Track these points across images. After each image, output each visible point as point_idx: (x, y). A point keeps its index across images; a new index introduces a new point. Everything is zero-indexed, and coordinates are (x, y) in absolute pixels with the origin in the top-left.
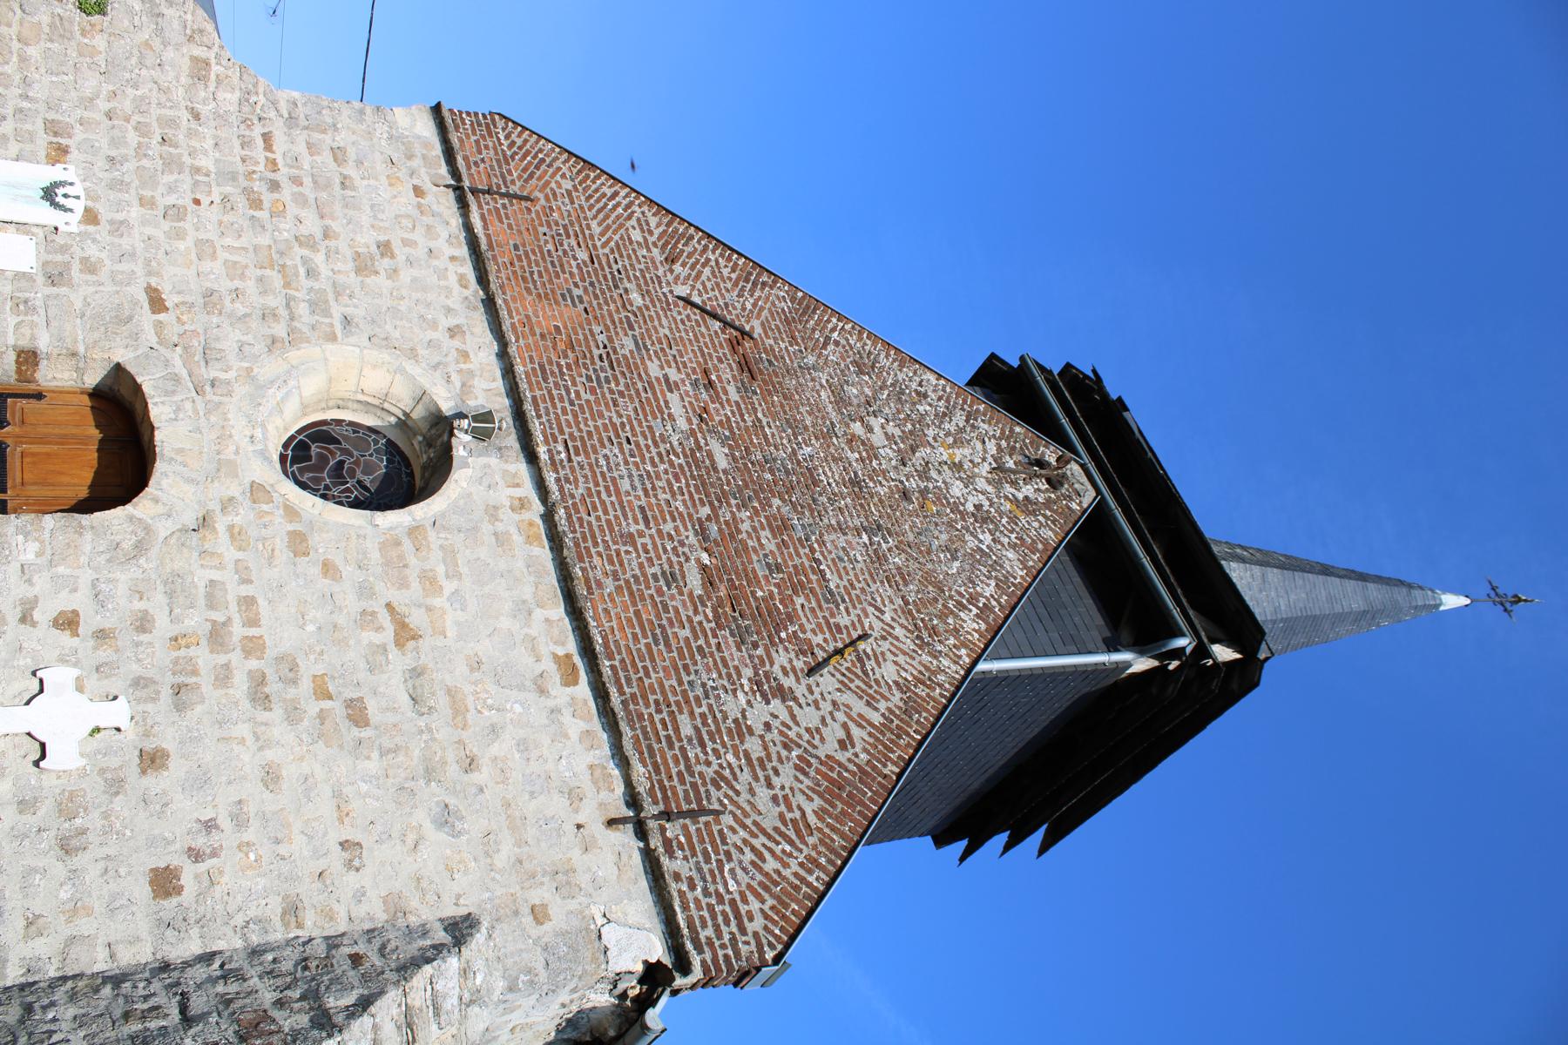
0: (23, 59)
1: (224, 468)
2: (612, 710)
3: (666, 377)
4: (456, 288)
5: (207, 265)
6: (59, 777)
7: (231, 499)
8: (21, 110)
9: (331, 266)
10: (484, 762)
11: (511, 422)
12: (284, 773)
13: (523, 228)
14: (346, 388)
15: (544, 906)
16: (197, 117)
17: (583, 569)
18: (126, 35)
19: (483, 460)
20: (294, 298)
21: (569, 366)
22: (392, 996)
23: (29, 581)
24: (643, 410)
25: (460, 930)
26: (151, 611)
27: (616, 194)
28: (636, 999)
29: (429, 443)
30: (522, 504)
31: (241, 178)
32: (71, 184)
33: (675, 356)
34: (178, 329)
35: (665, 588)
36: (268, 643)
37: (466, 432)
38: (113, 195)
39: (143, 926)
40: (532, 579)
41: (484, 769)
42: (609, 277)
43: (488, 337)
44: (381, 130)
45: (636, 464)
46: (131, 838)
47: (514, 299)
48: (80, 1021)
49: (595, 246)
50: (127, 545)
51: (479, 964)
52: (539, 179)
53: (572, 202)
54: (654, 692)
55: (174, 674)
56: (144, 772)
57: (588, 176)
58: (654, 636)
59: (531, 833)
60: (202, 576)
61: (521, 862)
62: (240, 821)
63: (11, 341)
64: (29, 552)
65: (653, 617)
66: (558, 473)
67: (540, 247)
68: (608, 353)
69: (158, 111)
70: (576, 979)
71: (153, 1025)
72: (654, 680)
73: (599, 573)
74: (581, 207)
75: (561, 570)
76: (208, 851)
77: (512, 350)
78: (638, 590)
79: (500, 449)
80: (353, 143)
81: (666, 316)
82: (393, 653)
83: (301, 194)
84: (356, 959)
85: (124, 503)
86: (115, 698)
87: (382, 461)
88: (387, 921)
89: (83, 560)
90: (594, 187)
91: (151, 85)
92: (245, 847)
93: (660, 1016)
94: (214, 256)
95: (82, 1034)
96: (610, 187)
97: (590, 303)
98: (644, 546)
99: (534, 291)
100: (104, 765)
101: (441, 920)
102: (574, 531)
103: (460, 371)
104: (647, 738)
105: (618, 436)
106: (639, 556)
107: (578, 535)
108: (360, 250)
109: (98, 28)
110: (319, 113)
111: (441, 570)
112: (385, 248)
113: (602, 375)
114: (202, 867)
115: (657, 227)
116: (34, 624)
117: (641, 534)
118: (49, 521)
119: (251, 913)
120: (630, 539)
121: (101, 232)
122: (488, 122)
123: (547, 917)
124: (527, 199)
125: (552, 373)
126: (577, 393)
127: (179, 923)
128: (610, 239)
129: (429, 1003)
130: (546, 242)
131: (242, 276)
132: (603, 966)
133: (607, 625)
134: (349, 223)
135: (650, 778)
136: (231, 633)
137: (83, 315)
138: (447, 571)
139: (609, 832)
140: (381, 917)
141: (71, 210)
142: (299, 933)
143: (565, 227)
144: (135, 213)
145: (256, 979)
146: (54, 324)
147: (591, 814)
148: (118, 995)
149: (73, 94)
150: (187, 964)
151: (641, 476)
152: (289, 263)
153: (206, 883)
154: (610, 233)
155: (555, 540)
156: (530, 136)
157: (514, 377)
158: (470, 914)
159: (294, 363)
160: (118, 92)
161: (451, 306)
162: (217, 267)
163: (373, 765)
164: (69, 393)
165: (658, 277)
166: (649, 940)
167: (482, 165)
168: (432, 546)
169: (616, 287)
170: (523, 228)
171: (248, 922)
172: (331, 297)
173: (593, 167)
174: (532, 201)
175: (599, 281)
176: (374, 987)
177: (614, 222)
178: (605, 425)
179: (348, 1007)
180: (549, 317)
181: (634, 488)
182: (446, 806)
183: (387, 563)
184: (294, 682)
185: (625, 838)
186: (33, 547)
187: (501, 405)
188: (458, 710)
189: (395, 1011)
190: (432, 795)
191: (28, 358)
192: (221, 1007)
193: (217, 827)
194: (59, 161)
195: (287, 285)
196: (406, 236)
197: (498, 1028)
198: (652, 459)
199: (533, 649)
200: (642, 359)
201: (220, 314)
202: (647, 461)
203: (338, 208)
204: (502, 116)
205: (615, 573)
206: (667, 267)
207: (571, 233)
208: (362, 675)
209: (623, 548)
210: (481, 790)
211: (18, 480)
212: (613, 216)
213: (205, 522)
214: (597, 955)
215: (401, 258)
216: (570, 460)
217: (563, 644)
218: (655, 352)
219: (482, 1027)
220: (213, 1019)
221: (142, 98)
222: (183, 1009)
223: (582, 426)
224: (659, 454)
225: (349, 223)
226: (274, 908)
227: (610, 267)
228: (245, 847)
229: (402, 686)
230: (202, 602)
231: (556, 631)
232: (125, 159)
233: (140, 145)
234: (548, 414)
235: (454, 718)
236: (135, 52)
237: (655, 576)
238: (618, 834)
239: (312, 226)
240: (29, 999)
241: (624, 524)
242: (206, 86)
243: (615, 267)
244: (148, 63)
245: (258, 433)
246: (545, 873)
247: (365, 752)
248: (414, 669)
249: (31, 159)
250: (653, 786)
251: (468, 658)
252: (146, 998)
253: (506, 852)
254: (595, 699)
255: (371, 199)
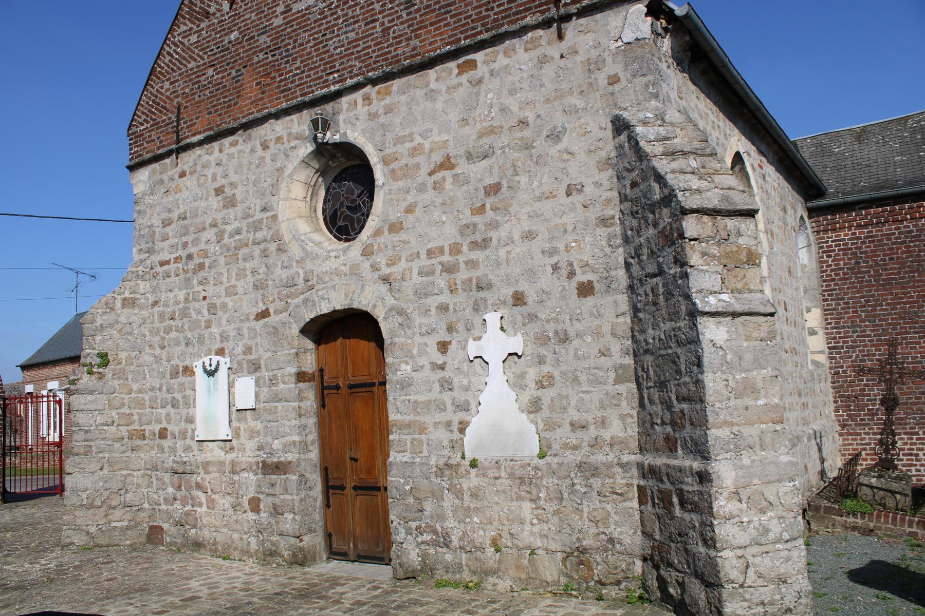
0: (140, 391)
1: (354, 271)
2: (491, 38)
3: (282, 13)
4: (239, 147)
5: (240, 290)
6: (527, 346)
7: (372, 266)
8: (168, 390)
9: (233, 221)
10: (522, 115)
11: (317, 108)
12: (527, 229)
13: (197, 110)
14: (304, 208)
15: (609, 77)
16: (156, 303)
17: (405, 60)
18: (117, 342)
19: (341, 124)
20: (254, 240)
21: (281, 75)
22: (655, 163)
23: (422, 367)
24: (304, 26)
25: (620, 126)
26: (436, 305)
27: (169, 53)
28: (668, 22)
29: (333, 157)
30: (367, 99)
31: (188, 276)
32: (204, 363)
33: (269, 9)
34: (277, 302)
35: (416, 7)
36: (453, 241)
37: (325, 135)
38: (207, 342)
39: (609, 299)
40: (412, 90)
41: (527, 114)
42: (222, 54)
43: (266, 125)
44: (148, 200)
45: (338, 30)
46: (561, 308)
47: (242, 112)
48: (655, 326)
49: (204, 64)
50: (400, 320)
51: (641, 115)
52: (165, 102)
53: (178, 81)
54: (481, 12)
55: (471, 291)
56: (525, 303)
57: (160, 72)
58: (446, 13)
59: (565, 86)
60: (416, 279)
61: (582, 92)
62: (553, 252)
63: (293, 385)
64: (406, 368)
65: (434, 15)
66: (347, 78)
67: (208, 99)
68: (270, 51)
69: (156, 323)
70: (654, 58)
71: (661, 290)
72: (473, 12)
73: (407, 49)
74: (180, 75)
75: (406, 73)
76: (570, 268)
77: (273, 110)
78: (417, 24)
79: (334, 114)
80: (159, 215)
81: (244, 16)
82: (458, 170)
83: (193, 242)
84: (634, 185)
85: (377, 323)
86: (485, 320)
87: (345, 184)
88: (613, 169)
89: (409, 341)
90: (166, 68)
91: (142, 328)
92: (568, 249)
93: (679, 6)
94: (234, 286)
95: (662, 325)
96: (165, 57)
97: (239, 65)
98: (389, 22)
99: (236, 100)
100: (521, 323)
101: (614, 139)
102: (382, 66)
103: (289, 141)
104: (509, 16)
105: (322, 42)
106: (396, 25)
107: (384, 63)
108: (222, 205)
109: (115, 356)
110: (143, 236)
111: (408, 145)
112: (219, 191)
113: (284, 54)
114: (578, 271)
115: (186, 25)
116: (445, 363)
117: (382, 24)
118: (389, 360)
119: (605, 243)
120: (385, 31)
121: (228, 346)
122: (135, 137)
123: (616, 75)
124: (179, 109)
125: (285, 85)
126: (296, 69)
127: (608, 281)
128: (198, 55)
129: (661, 143)
130: (204, 95)
131: (244, 270)
132: (647, 41)
133: (439, 43)
134: (206, 213)
135: (534, 13)
136: (448, 262)
137: (275, 351)
138: (409, 141)
139: (566, 38)
140: (611, 172)
141: (218, 362)
142: (617, 217)
143: (194, 84)
144: (215, 330)
145: (641, 239)
146: (281, 365)
147: (554, 51)
148: (644, 310)
149: (154, 366)
150: (630, 276)
151: (346, 26)
152: (233, 245)
153: (587, 268)
154: (194, 55)
155: (388, 77)
156: (139, 110)
157: (290, 108)
158: (611, 121)
159: (291, 237)
160: (149, 344)
161: (249, 149)
162: (240, 285)
163: (523, 179)
164: (318, 356)
165: (219, 22)
166: (633, 13)
167: (161, 138)
168: (394, 151)
169: (228, 49)
170: (197, 110)
171: (610, 245)
172: (251, 220)
173: (153, 69)
174: (180, 106)
175: (226, 60)
176: (651, 173)
177: (187, 53)
178: (315, 51)
179: (660, 188)
180: (251, 90)
181: (354, 30)
182: (547, 136)
183: (406, 176)
184: (475, 225)
185: (570, 29)
186: (403, 367)
187: (307, 116)
188: (491, 131)
189: (665, 162)
190: (541, 145)
191: (301, 377)
192: (655, 256)
193: (556, 264)
194: (192, 370)
195: (246, 245)
196: (210, 179)
197: (679, 106)
198: (335, 19)
199: (454, 88)
200: (272, 29)
201: (266, 280)
202: (336, 22)
203: (198, 220)
204: (129, 129)
205: (408, 39)
206: (212, 17)
207: (197, 80)
208: (471, 187)
209: (392, 35)
210: (539, 116)
211: (368, 377)
212: (183, 54)
213: (386, 279)
214: (640, 45)
215: (224, 181)
216: (338, 71)
217: (451, 70)
218: (267, 21)
219: (677, 114)
220: (661, 260)
221: (150, 332)
222: (654, 275)
223: (317, 65)
224: (332, 15)
225: (206, 213)
226: (602, 232)
227: (216, 54)
228: (568, 249)
229: (477, 164)
230: (430, 278)
231: (444, 75)
232: (186, 337)
233: (177, 331)
234: (311, 86)
235: (496, 133)
236: (125, 337)
237: (408, 14)
238: (567, 33)
239: (210, 234)
240: (642, 351)
241: (376, 35)
242: (138, 299)
243: (215, 51)
244: (130, 330)
245: (333, 254)
246: (589, 77)
247: (515, 184)
248: (467, 158)
249: (193, 383)
250: (538, 12)
251: (460, 127)
252: (647, 295)
253: (576, 101)
254: (485, 49)
255: (191, 202)
